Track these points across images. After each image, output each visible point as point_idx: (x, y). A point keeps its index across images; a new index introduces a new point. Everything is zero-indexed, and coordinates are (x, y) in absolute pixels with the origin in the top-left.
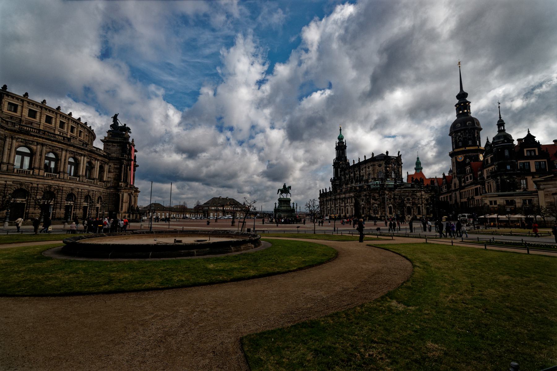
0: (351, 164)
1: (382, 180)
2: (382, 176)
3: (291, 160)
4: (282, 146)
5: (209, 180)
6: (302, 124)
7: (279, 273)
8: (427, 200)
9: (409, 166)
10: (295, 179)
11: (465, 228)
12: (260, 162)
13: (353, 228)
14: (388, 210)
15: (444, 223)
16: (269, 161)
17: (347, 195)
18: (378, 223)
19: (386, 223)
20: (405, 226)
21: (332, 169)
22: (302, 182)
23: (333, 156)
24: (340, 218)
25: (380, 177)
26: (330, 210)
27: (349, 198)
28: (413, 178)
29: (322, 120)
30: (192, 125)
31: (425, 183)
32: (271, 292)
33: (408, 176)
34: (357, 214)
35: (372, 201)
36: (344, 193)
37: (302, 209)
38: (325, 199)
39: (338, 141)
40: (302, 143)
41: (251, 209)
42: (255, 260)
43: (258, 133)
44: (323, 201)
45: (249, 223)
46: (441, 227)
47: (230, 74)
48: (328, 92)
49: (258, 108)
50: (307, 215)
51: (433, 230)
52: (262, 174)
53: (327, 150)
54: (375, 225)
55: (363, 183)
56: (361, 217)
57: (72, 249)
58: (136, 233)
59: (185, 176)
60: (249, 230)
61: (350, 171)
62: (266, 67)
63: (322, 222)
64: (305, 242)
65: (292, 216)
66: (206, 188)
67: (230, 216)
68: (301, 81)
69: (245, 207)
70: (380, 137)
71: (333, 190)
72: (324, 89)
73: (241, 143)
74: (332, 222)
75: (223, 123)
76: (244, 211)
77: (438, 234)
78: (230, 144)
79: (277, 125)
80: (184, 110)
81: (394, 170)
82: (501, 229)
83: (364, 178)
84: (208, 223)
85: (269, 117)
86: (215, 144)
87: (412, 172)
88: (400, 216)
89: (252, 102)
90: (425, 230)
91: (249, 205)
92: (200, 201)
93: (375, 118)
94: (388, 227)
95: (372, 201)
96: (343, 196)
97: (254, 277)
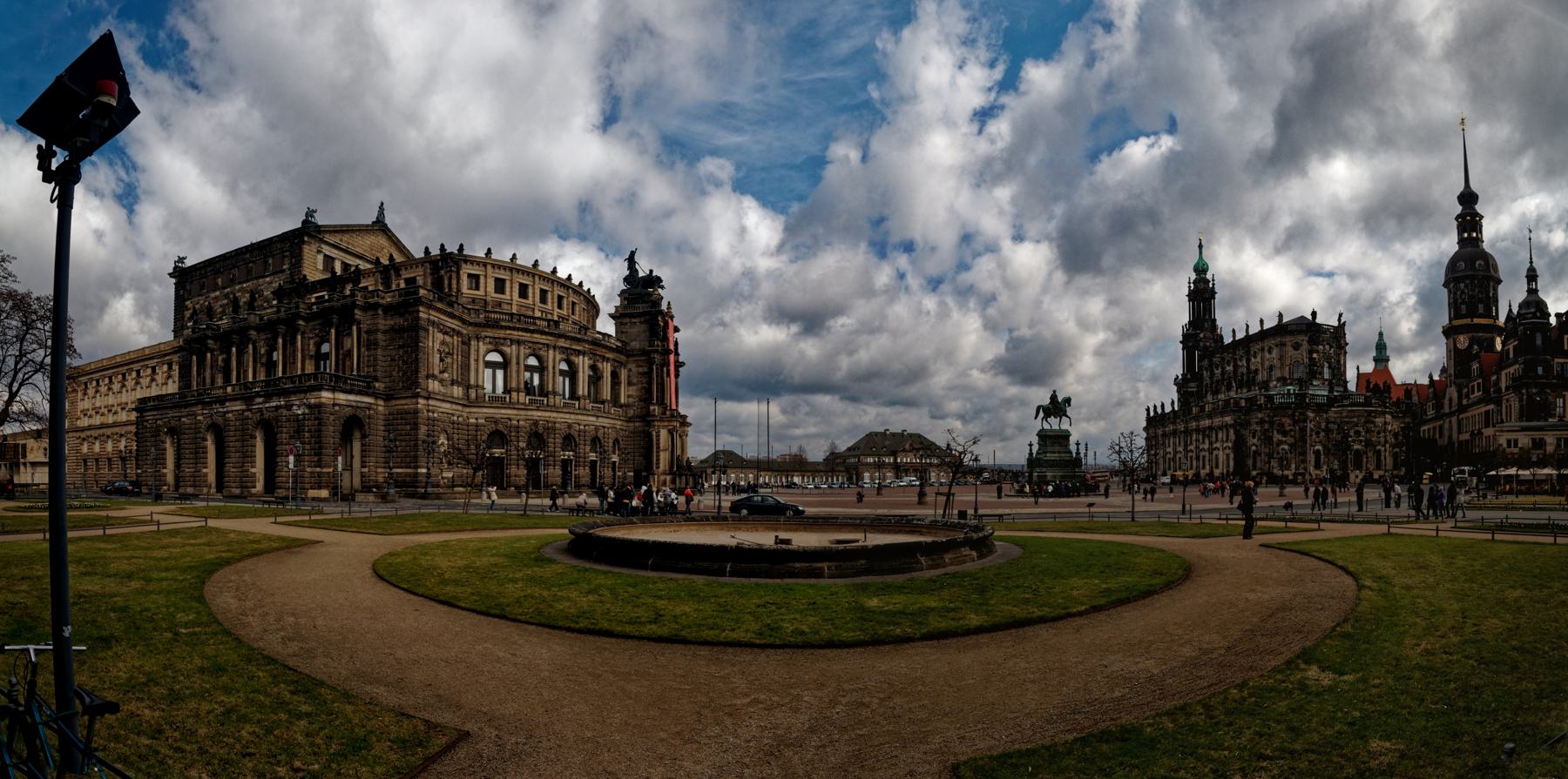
0: (1228, 340)
1: (1300, 382)
2: (1300, 373)
3: (1070, 328)
4: (1046, 289)
5: (856, 388)
6: (1099, 226)
7: (1042, 620)
8: (1396, 435)
9: (1361, 352)
10: (1083, 376)
11: (1462, 498)
12: (988, 333)
13: (1228, 506)
14: (1311, 458)
15: (1426, 488)
16: (1011, 331)
17: (1217, 421)
18: (1289, 490)
19: (1307, 490)
20: (1347, 497)
21: (1178, 351)
22: (1099, 386)
23: (1181, 315)
24: (1197, 480)
25: (1296, 376)
26: (1174, 459)
27: (1221, 428)
28: (1368, 382)
29: (1153, 217)
30: (809, 247)
31: (1395, 395)
32: (1023, 665)
33: (1359, 376)
34: (1241, 470)
35: (1277, 437)
36: (1210, 416)
37: (1100, 457)
38: (1160, 432)
39: (1193, 277)
40: (1098, 280)
41: (967, 460)
42: (982, 590)
43: (979, 255)
44: (1156, 436)
45: (964, 497)
46: (1420, 494)
47: (903, 99)
48: (1167, 142)
49: (978, 186)
50: (1114, 473)
51: (1404, 505)
52: (992, 368)
53: (1164, 301)
54: (1281, 495)
55: (1255, 391)
56: (1247, 477)
57: (585, 547)
58: (693, 519)
59: (797, 379)
60: (963, 514)
61: (1223, 359)
62: (998, 73)
63: (1153, 492)
64: (1107, 543)
65: (1074, 477)
66: (851, 408)
67: (912, 479)
68: (1096, 107)
69: (951, 455)
70: (1299, 272)
71: (1180, 408)
72: (1156, 133)
73: (934, 284)
74: (1178, 490)
75: (887, 233)
76: (949, 465)
77: (1413, 513)
78: (907, 289)
79: (1032, 229)
80: (790, 211)
81: (1328, 359)
82: (1522, 498)
83: (1260, 377)
84: (860, 497)
85: (1007, 208)
86: (868, 292)
87: (1368, 367)
88: (1339, 473)
89: (962, 171)
90: (1388, 506)
91: (960, 449)
92: (837, 442)
93: (1286, 221)
94: (1310, 501)
95: (1277, 437)
96: (1207, 422)
97: (979, 630)
